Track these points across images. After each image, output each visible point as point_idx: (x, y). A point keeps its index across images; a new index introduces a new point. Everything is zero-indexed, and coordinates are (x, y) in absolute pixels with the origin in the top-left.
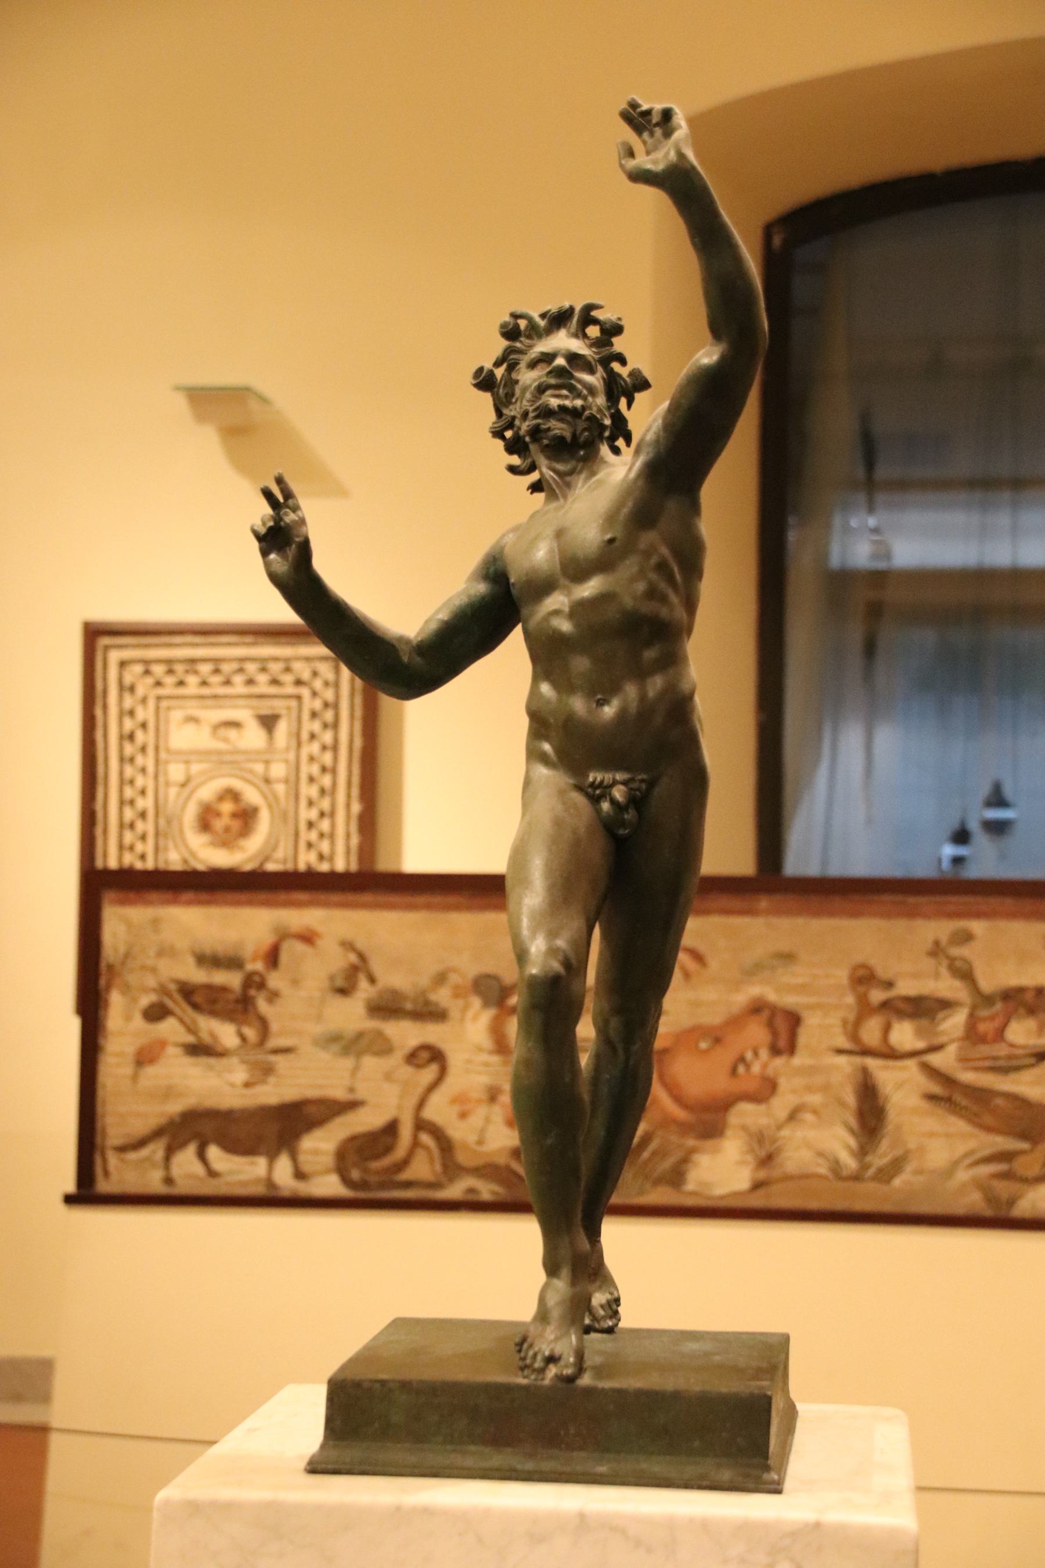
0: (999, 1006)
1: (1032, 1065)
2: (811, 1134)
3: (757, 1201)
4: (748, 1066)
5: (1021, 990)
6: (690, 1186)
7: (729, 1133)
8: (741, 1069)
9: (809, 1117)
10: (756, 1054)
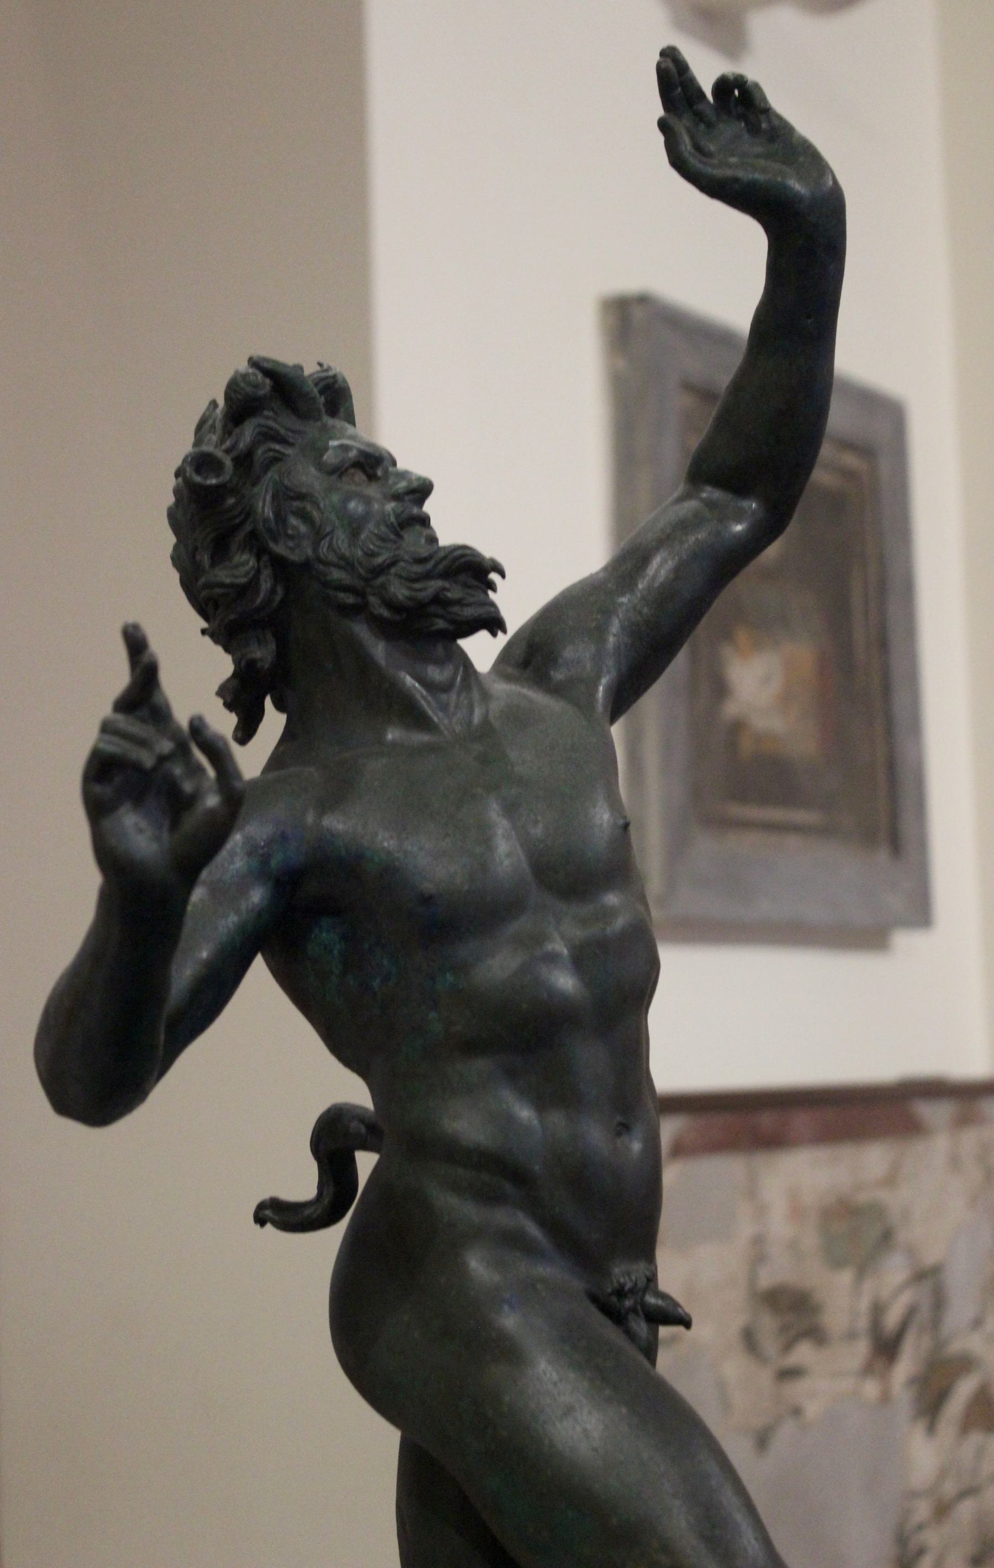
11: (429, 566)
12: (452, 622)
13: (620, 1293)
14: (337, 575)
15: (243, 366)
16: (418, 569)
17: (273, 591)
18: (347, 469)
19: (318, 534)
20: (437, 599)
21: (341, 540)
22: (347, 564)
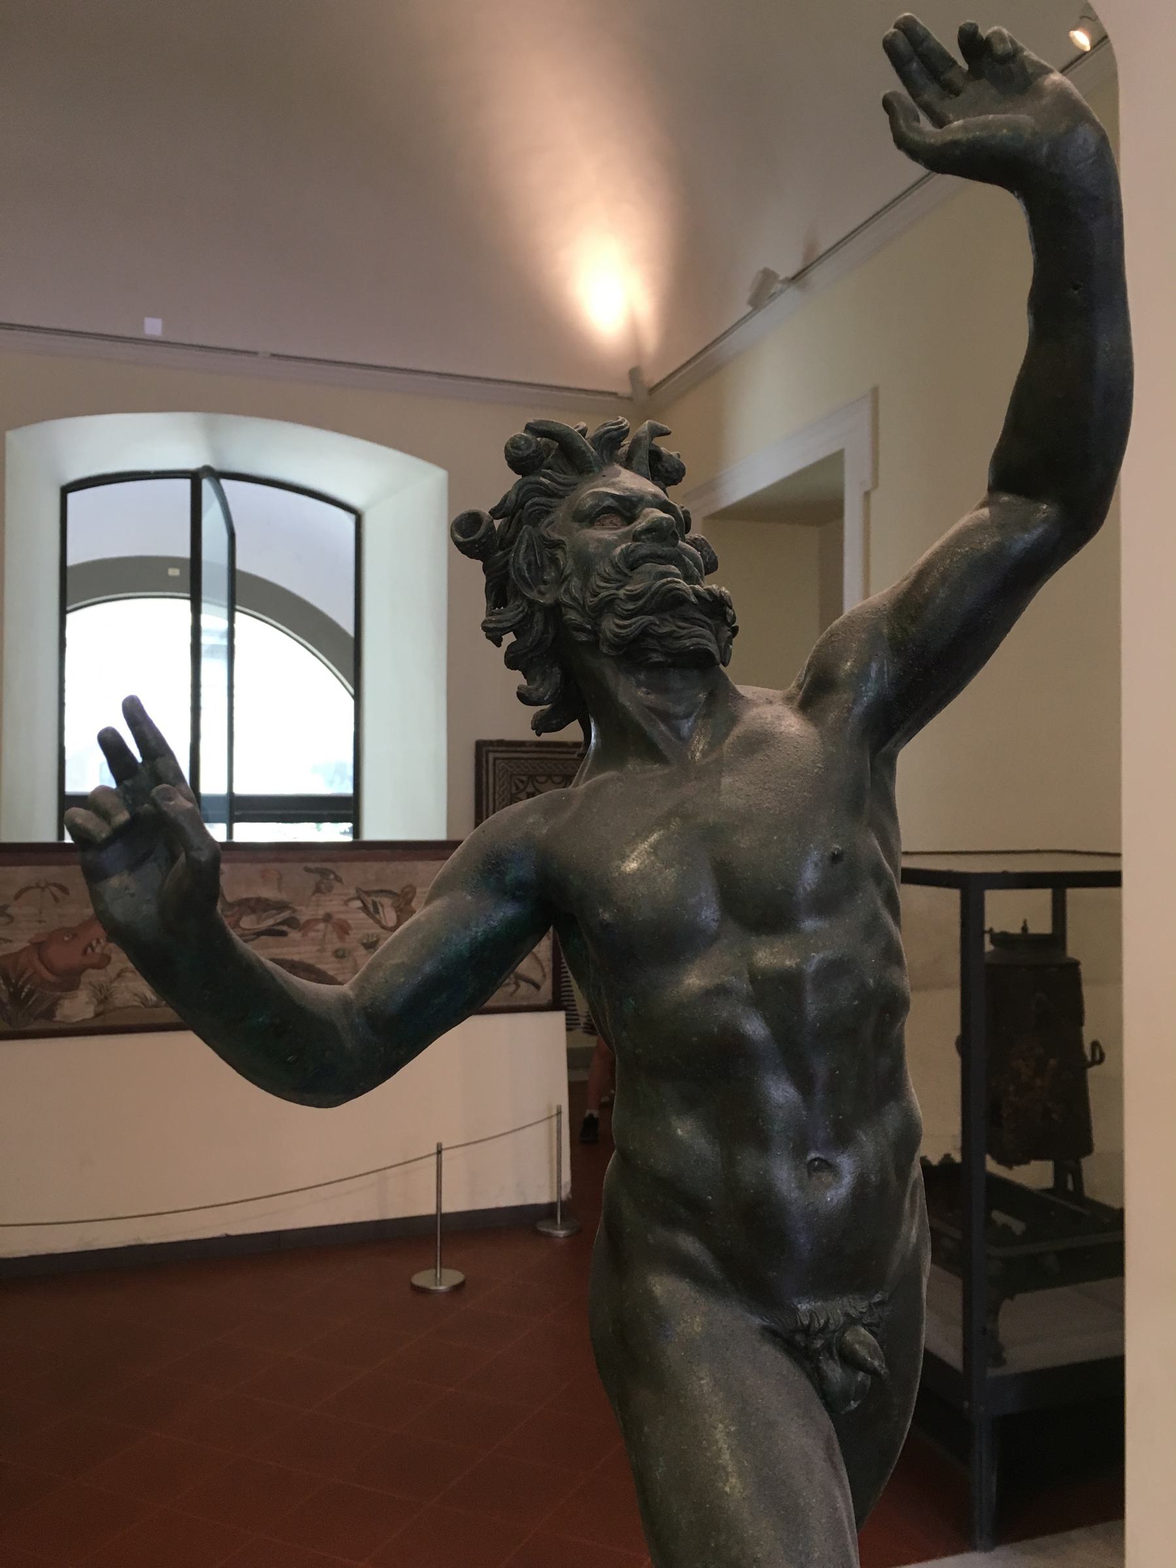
0: (236, 909)
1: (253, 940)
2: (130, 984)
3: (97, 1023)
4: (93, 950)
5: (248, 900)
6: (58, 1018)
7: (82, 986)
8: (89, 950)
9: (129, 975)
10: (98, 942)
11: (641, 602)
12: (667, 654)
13: (806, 1331)
14: (572, 616)
15: (520, 431)
16: (631, 606)
17: (545, 631)
18: (598, 514)
19: (562, 579)
20: (645, 633)
21: (575, 583)
22: (581, 608)
